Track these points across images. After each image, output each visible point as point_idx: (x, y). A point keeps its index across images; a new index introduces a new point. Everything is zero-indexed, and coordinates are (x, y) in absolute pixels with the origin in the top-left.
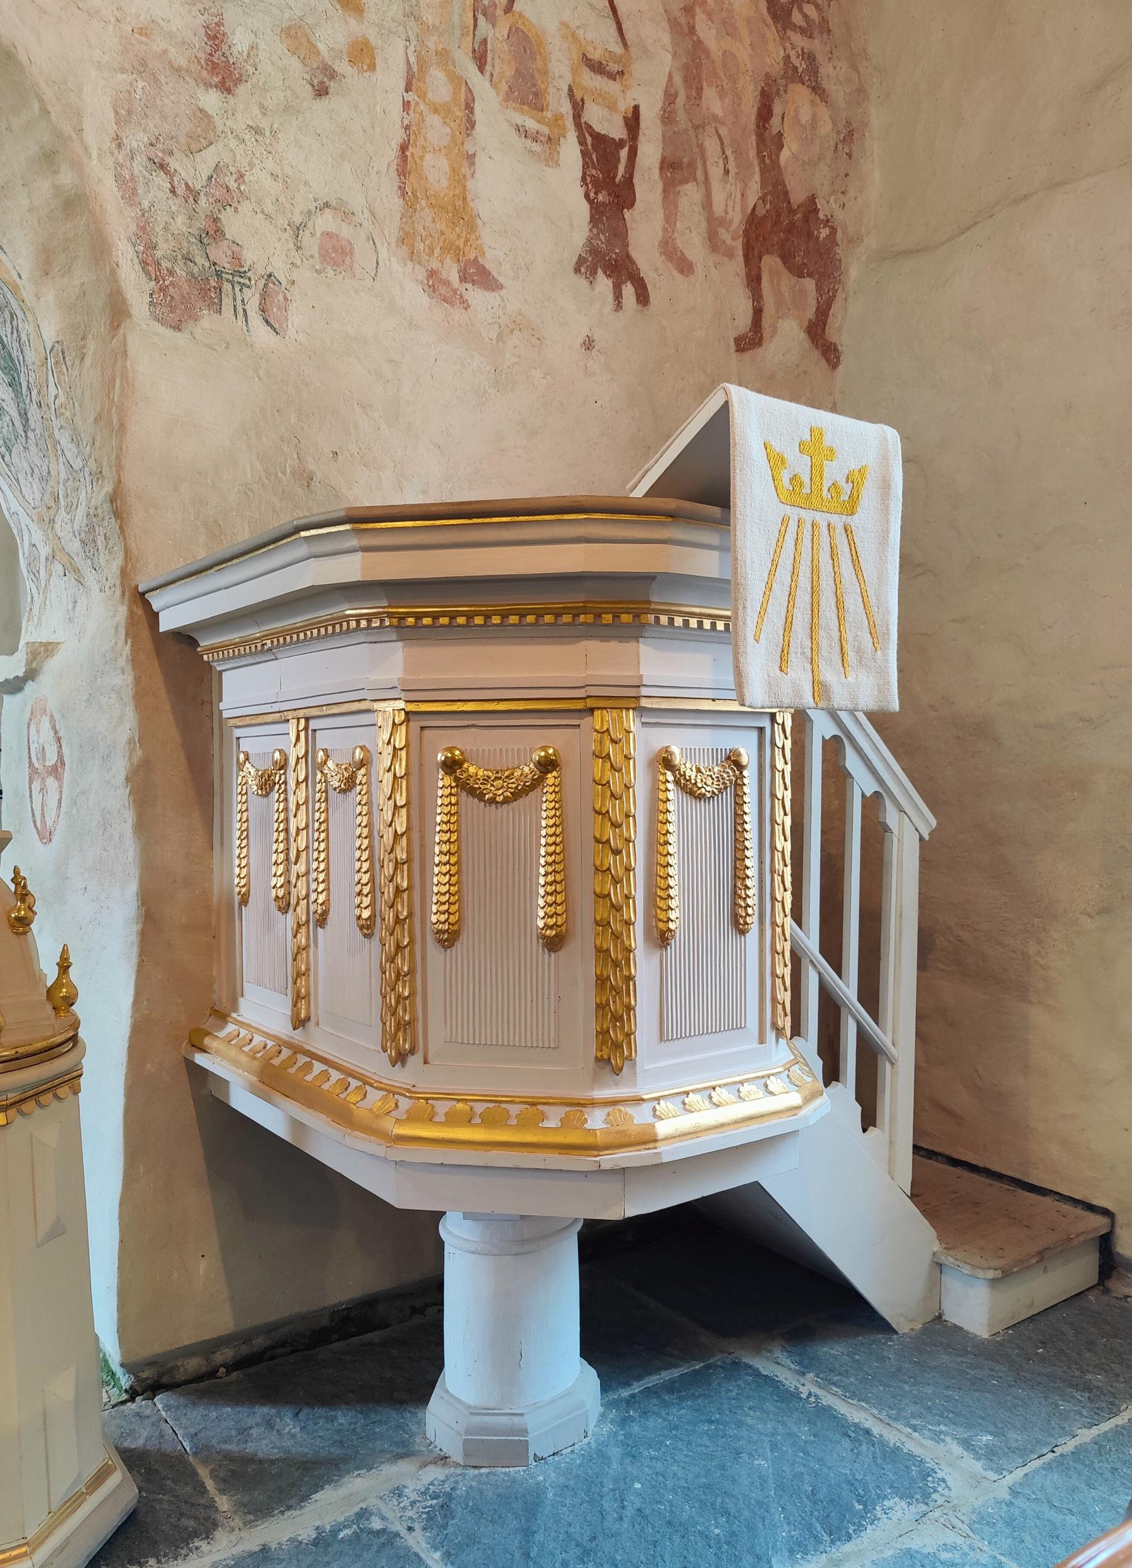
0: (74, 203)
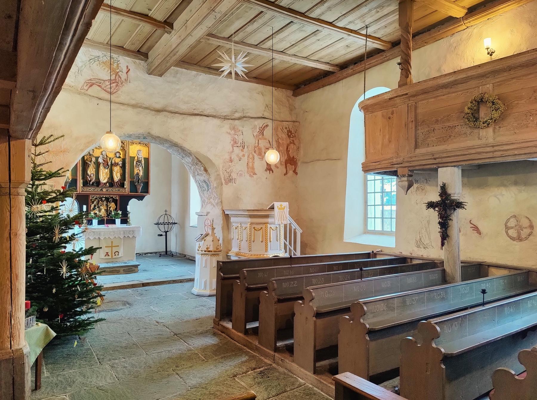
0: (218, 175)
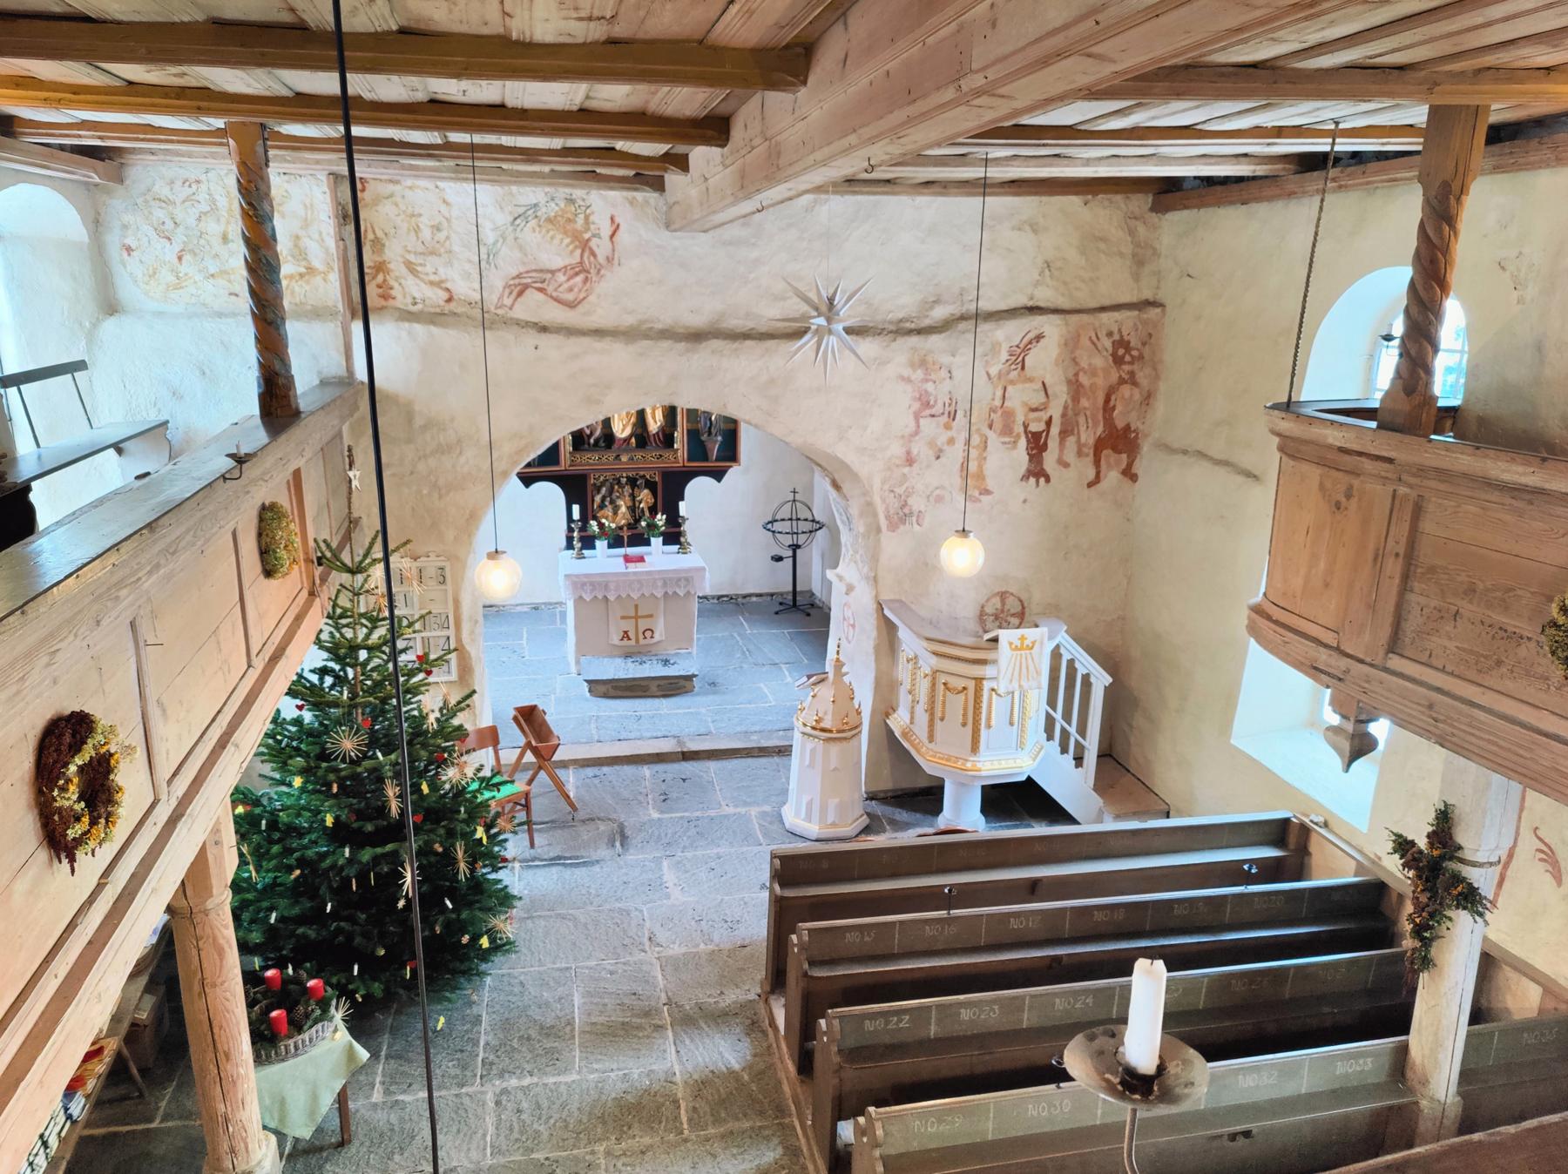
0: (870, 504)
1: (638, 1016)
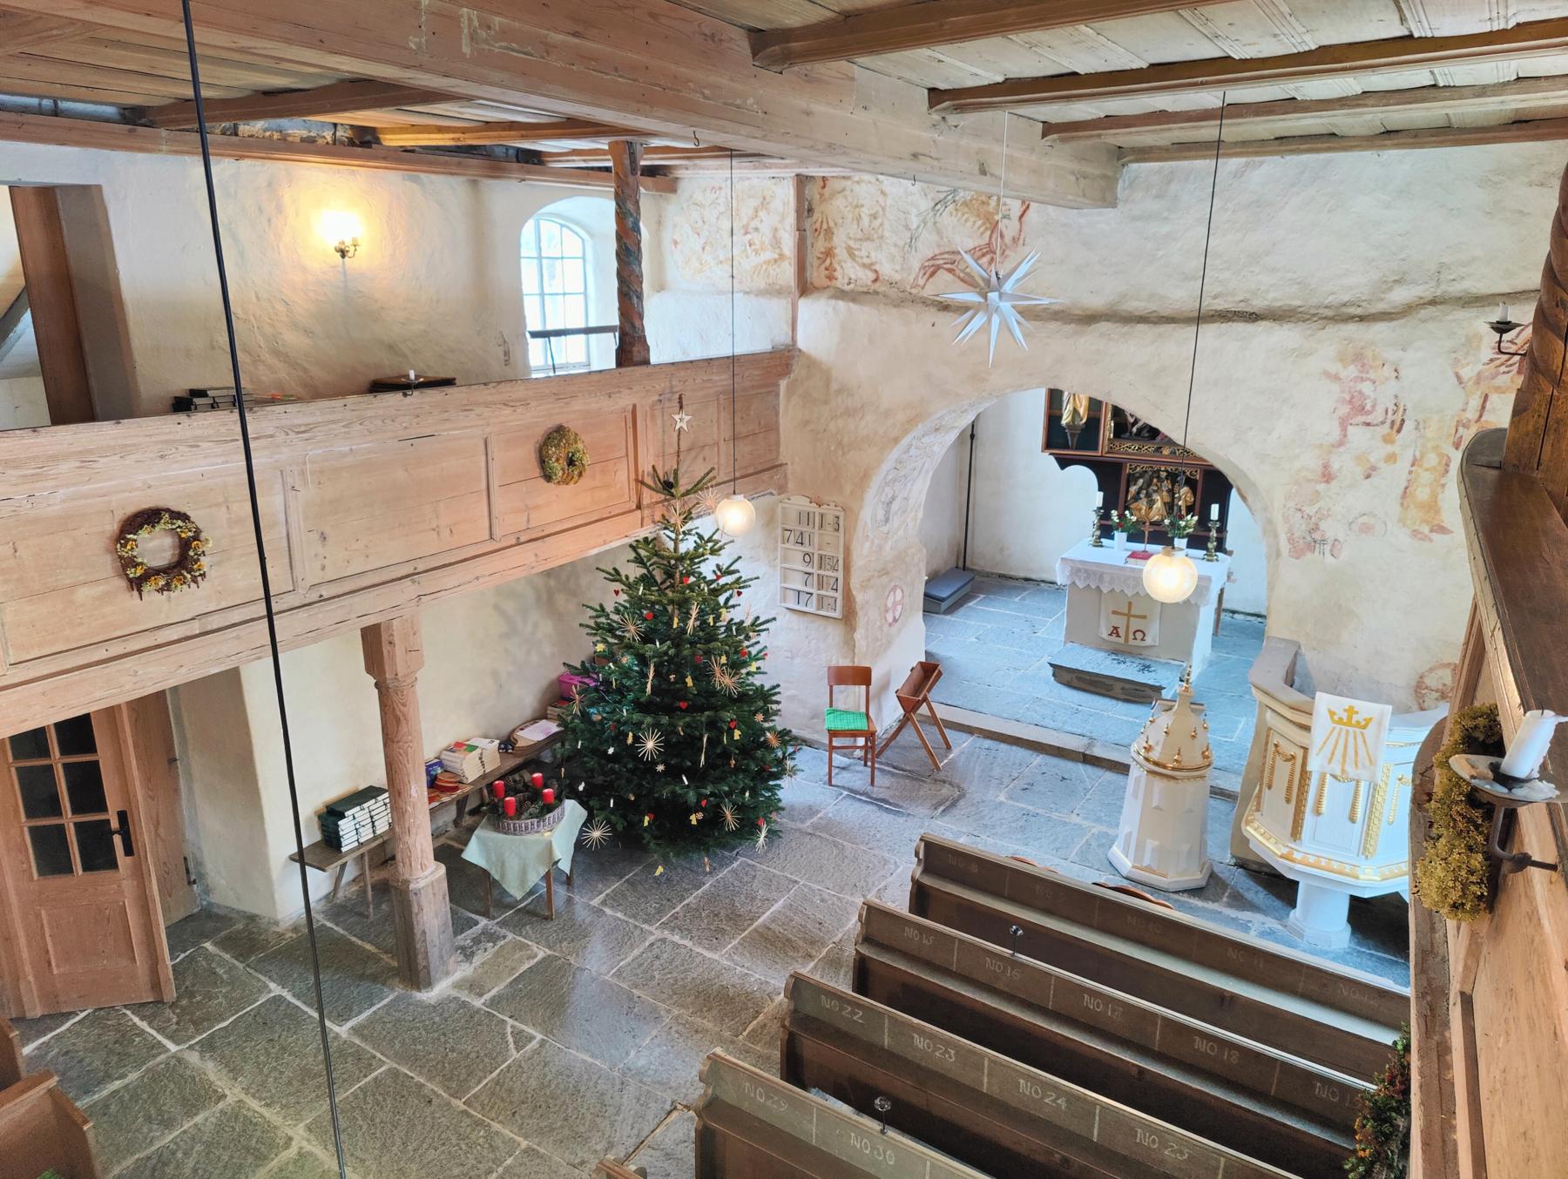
0: (1270, 521)
1: (805, 940)
